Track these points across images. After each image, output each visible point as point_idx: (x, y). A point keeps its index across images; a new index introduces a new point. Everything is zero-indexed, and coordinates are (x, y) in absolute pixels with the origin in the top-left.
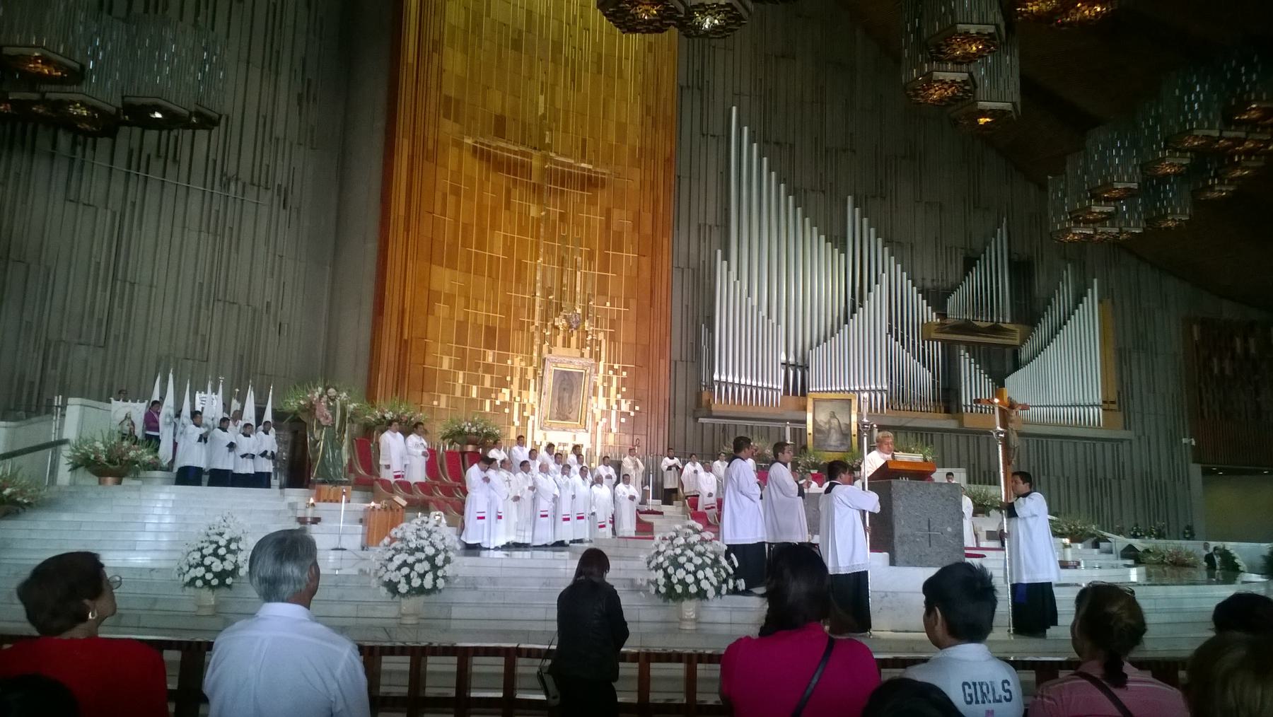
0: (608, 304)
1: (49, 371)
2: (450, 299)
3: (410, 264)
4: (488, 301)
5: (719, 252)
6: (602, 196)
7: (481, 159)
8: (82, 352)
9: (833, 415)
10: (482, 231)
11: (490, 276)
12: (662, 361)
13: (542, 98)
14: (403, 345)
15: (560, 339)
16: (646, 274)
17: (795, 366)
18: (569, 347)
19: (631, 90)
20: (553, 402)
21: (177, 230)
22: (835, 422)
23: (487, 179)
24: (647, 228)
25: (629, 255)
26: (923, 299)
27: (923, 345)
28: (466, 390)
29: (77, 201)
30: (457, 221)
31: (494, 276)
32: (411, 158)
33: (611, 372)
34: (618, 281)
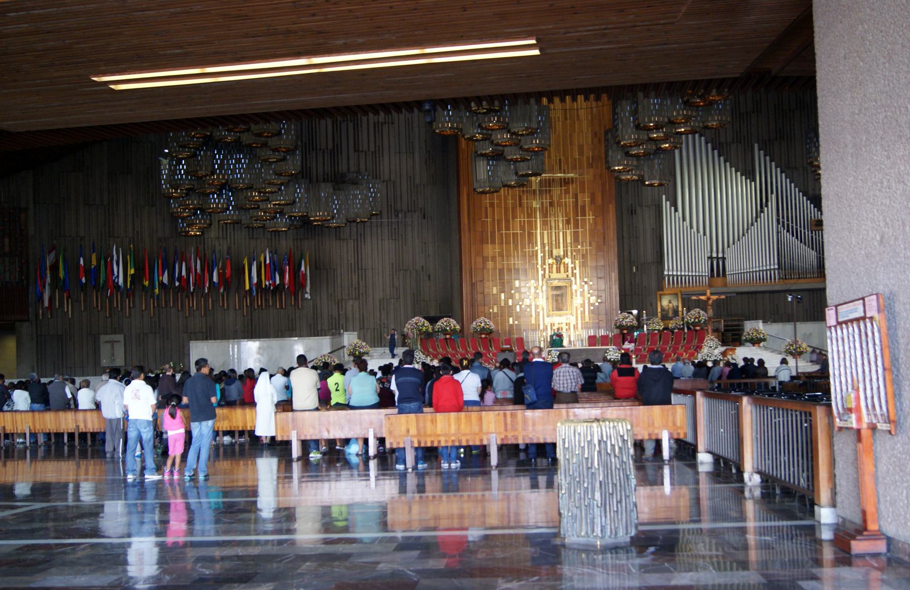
0: (579, 247)
1: (341, 312)
2: (494, 259)
3: (472, 247)
5: (664, 196)
8: (351, 302)
9: (670, 302)
10: (507, 221)
12: (613, 274)
14: (473, 285)
16: (600, 227)
17: (718, 258)
19: (585, 125)
20: (552, 303)
21: (380, 241)
22: (671, 305)
23: (508, 194)
25: (590, 217)
26: (811, 203)
27: (812, 233)
28: (506, 302)
29: (340, 239)
30: (494, 220)
32: (468, 195)
33: (583, 283)
34: (585, 231)
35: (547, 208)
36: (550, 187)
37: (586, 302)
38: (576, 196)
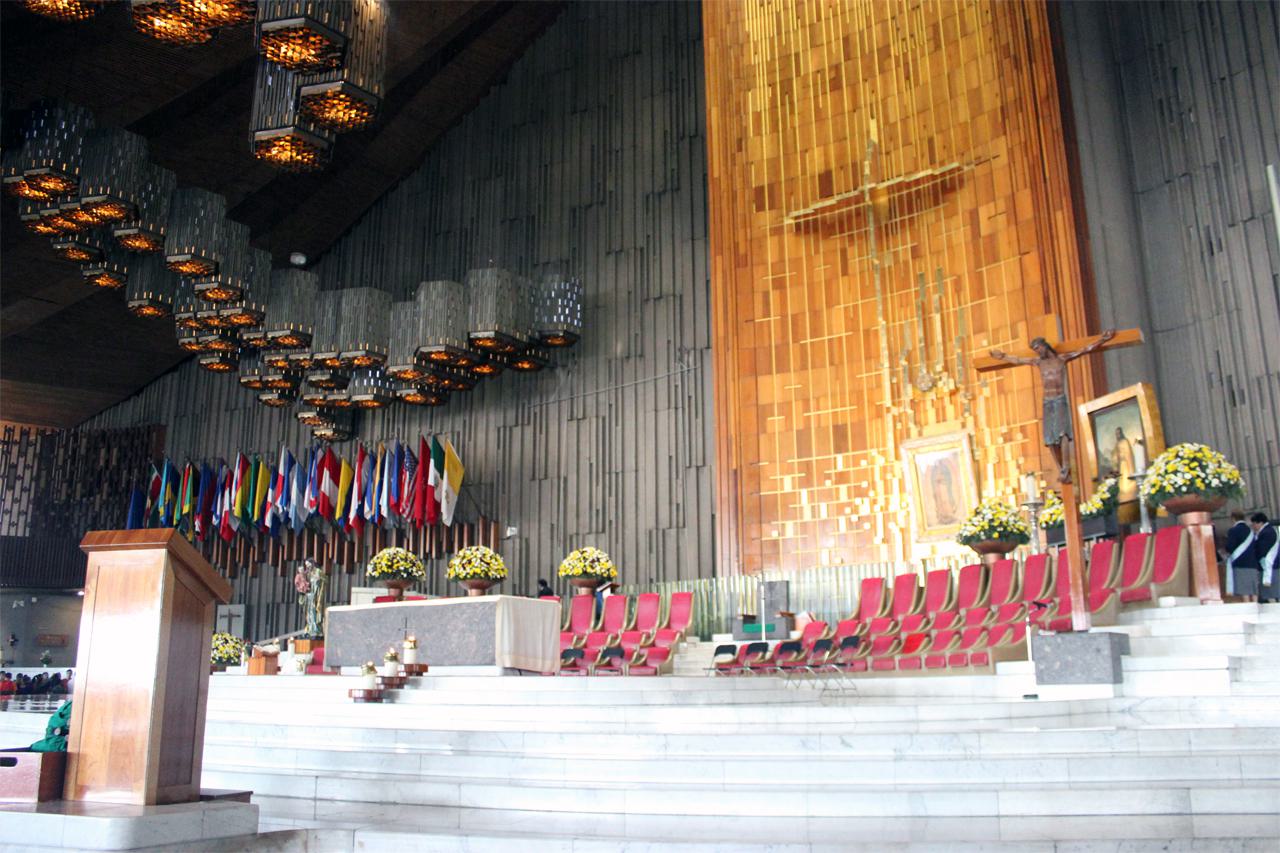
2: (785, 409)
4: (833, 395)
6: (963, 200)
7: (807, 232)
10: (815, 314)
11: (831, 364)
13: (873, 124)
15: (931, 414)
16: (1034, 276)
18: (944, 420)
23: (817, 252)
24: (1026, 208)
30: (784, 316)
31: (836, 361)
35: (906, 263)
36: (911, 211)
37: (1009, 490)
38: (974, 215)
